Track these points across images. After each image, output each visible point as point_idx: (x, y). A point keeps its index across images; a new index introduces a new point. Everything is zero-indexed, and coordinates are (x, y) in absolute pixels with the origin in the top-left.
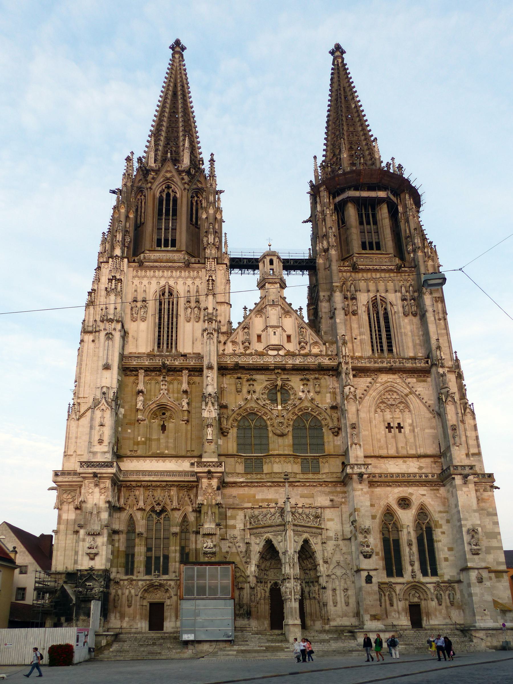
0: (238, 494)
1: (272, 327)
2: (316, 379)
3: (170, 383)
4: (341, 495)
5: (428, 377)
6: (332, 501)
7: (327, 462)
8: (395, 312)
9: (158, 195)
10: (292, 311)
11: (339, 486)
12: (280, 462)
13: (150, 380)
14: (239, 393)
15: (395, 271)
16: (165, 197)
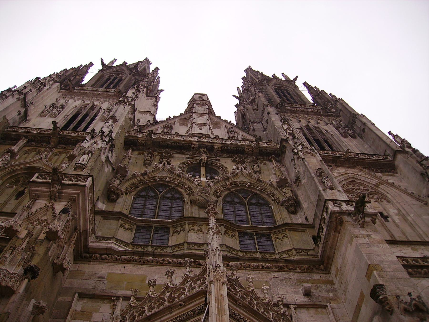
0: (109, 274)
1: (197, 124)
2: (254, 161)
3: (56, 154)
4: (323, 286)
5: (393, 172)
6: (307, 294)
7: (286, 236)
8: (332, 135)
9: (107, 77)
10: (221, 122)
11: (315, 270)
12: (201, 230)
13: (30, 150)
14: (147, 166)
15: (322, 113)
16: (113, 78)
